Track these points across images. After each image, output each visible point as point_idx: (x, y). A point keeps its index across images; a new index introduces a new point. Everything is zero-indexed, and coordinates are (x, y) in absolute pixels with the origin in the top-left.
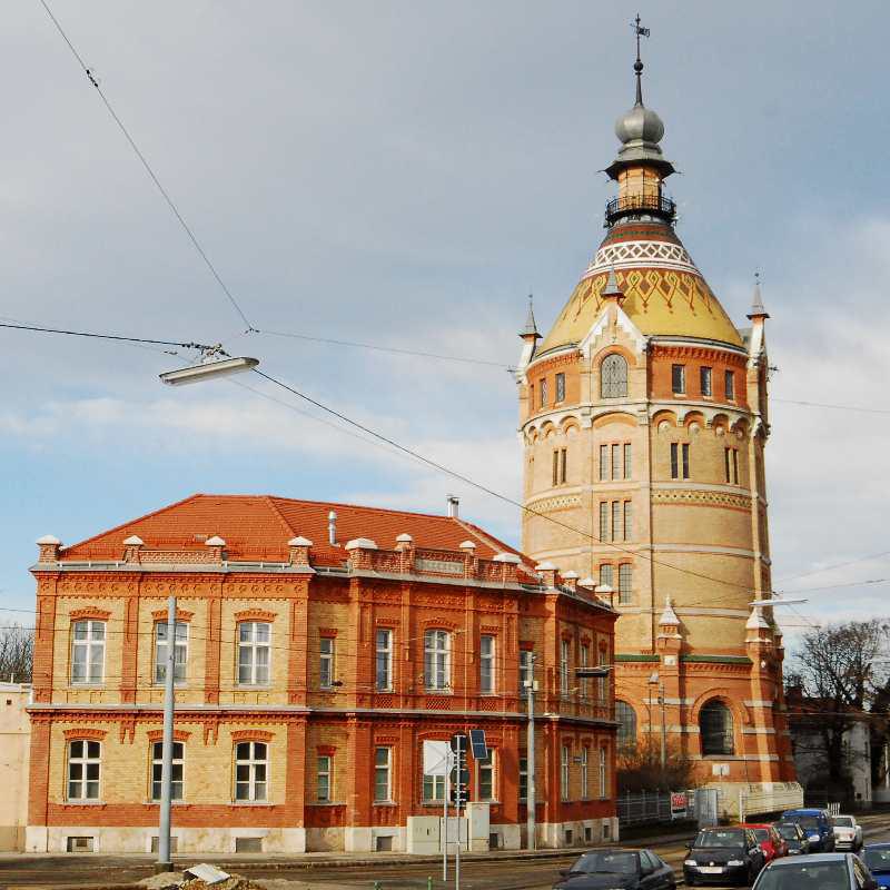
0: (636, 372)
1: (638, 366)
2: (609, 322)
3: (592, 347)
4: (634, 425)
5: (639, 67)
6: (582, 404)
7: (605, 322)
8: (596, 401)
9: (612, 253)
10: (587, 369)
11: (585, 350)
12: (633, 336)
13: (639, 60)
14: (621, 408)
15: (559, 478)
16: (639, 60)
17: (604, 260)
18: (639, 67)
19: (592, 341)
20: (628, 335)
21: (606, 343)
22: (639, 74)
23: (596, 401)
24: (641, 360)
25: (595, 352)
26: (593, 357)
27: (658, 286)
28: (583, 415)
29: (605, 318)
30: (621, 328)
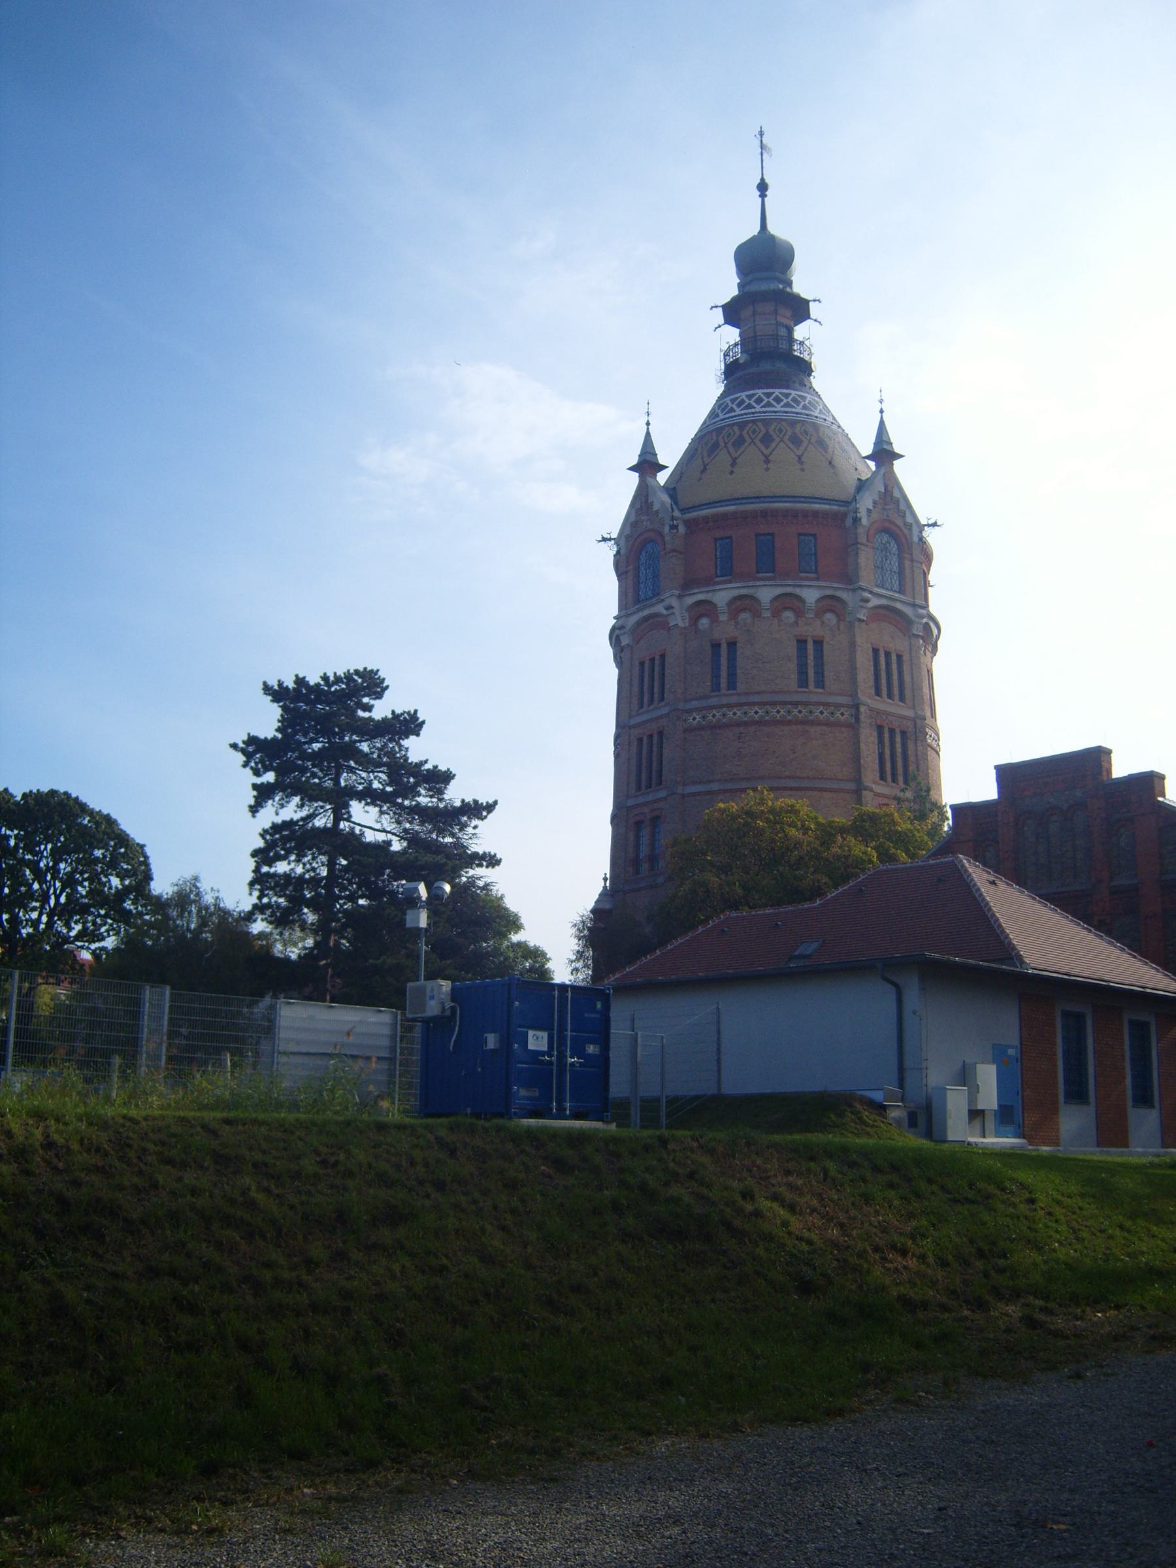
5: (763, 187)
9: (727, 406)
13: (762, 179)
16: (762, 179)
17: (717, 416)
18: (763, 187)
22: (763, 196)
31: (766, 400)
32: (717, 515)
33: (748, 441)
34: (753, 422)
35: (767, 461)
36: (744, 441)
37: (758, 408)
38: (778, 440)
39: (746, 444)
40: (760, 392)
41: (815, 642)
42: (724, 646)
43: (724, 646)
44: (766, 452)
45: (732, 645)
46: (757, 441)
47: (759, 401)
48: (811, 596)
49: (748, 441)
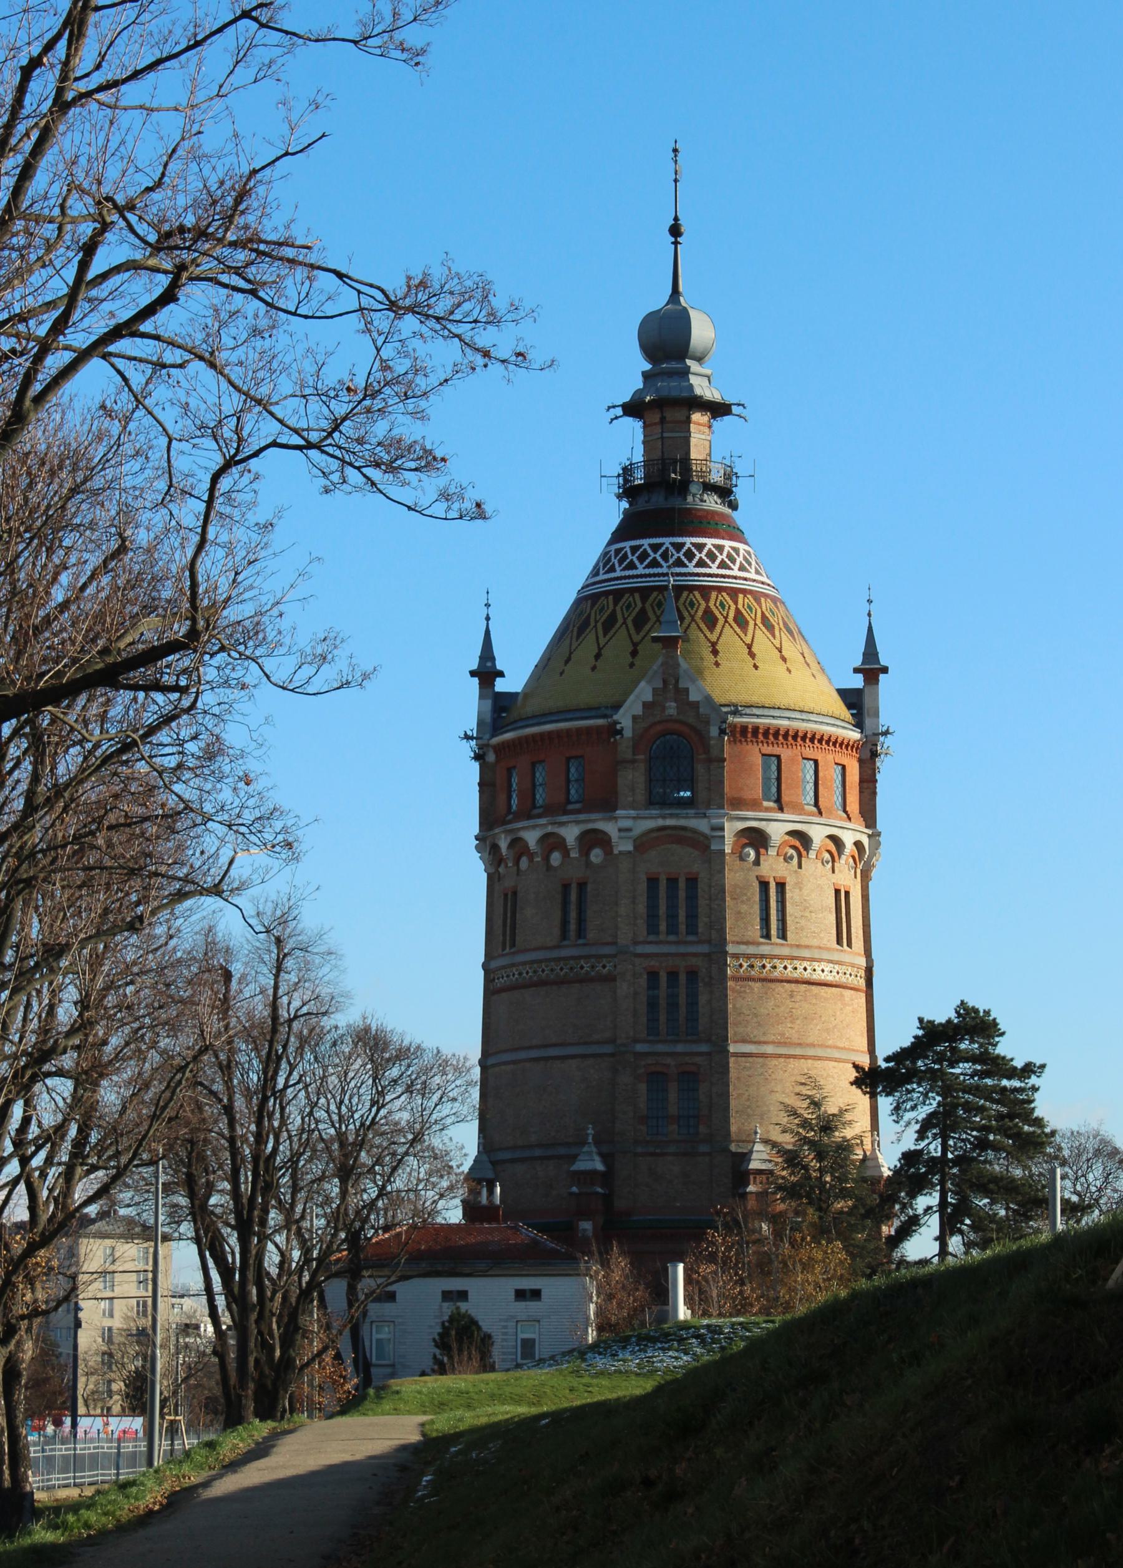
5: (675, 231)
15: (573, 926)
16: (676, 219)
18: (675, 231)
22: (676, 243)
28: (620, 830)
31: (652, 555)
32: (527, 737)
33: (620, 621)
34: (632, 591)
37: (641, 570)
39: (618, 625)
40: (646, 543)
41: (777, 884)
42: (574, 886)
43: (574, 886)
45: (582, 886)
47: (643, 557)
48: (571, 834)
49: (620, 621)
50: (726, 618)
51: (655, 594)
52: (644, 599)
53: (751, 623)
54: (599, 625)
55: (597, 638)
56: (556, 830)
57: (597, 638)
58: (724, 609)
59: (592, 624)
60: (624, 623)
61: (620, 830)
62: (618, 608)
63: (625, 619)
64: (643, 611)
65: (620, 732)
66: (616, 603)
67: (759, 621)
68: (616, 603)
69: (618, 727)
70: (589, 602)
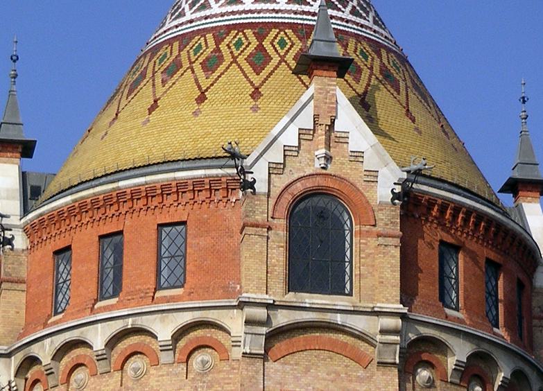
0: (373, 242)
1: (379, 229)
2: (316, 117)
3: (275, 169)
4: (358, 358)
6: (246, 296)
7: (306, 121)
8: (278, 293)
10: (260, 218)
11: (259, 174)
12: (370, 162)
14: (339, 319)
19: (276, 155)
20: (357, 156)
21: (310, 163)
23: (278, 293)
24: (389, 219)
25: (280, 182)
26: (275, 192)
27: (376, 70)
29: (310, 111)
30: (343, 139)
33: (228, 59)
34: (241, 27)
35: (256, 94)
36: (221, 59)
38: (276, 59)
39: (225, 64)
44: (256, 80)
46: (241, 59)
49: (228, 59)
50: (371, 69)
51: (274, 32)
52: (260, 37)
53: (402, 84)
54: (197, 67)
55: (196, 81)
56: (143, 322)
57: (196, 81)
58: (367, 60)
59: (186, 64)
60: (235, 59)
61: (248, 322)
62: (223, 47)
63: (235, 59)
64: (261, 48)
65: (251, 185)
66: (218, 41)
67: (409, 84)
68: (218, 41)
69: (249, 178)
70: (176, 45)
